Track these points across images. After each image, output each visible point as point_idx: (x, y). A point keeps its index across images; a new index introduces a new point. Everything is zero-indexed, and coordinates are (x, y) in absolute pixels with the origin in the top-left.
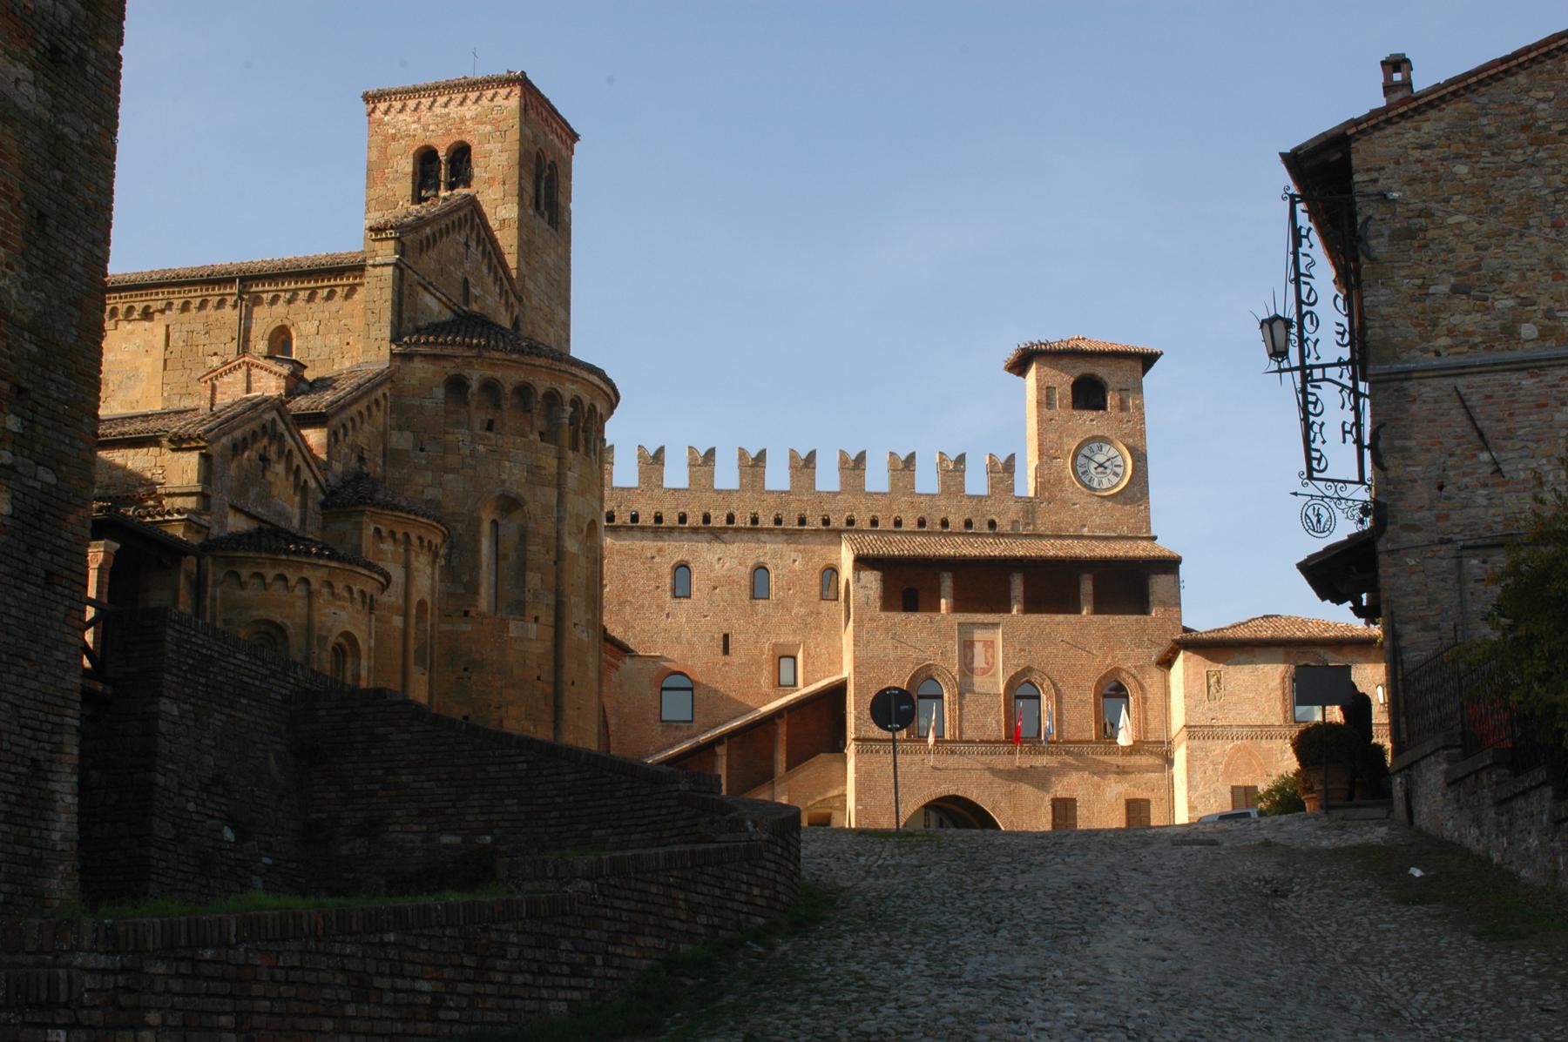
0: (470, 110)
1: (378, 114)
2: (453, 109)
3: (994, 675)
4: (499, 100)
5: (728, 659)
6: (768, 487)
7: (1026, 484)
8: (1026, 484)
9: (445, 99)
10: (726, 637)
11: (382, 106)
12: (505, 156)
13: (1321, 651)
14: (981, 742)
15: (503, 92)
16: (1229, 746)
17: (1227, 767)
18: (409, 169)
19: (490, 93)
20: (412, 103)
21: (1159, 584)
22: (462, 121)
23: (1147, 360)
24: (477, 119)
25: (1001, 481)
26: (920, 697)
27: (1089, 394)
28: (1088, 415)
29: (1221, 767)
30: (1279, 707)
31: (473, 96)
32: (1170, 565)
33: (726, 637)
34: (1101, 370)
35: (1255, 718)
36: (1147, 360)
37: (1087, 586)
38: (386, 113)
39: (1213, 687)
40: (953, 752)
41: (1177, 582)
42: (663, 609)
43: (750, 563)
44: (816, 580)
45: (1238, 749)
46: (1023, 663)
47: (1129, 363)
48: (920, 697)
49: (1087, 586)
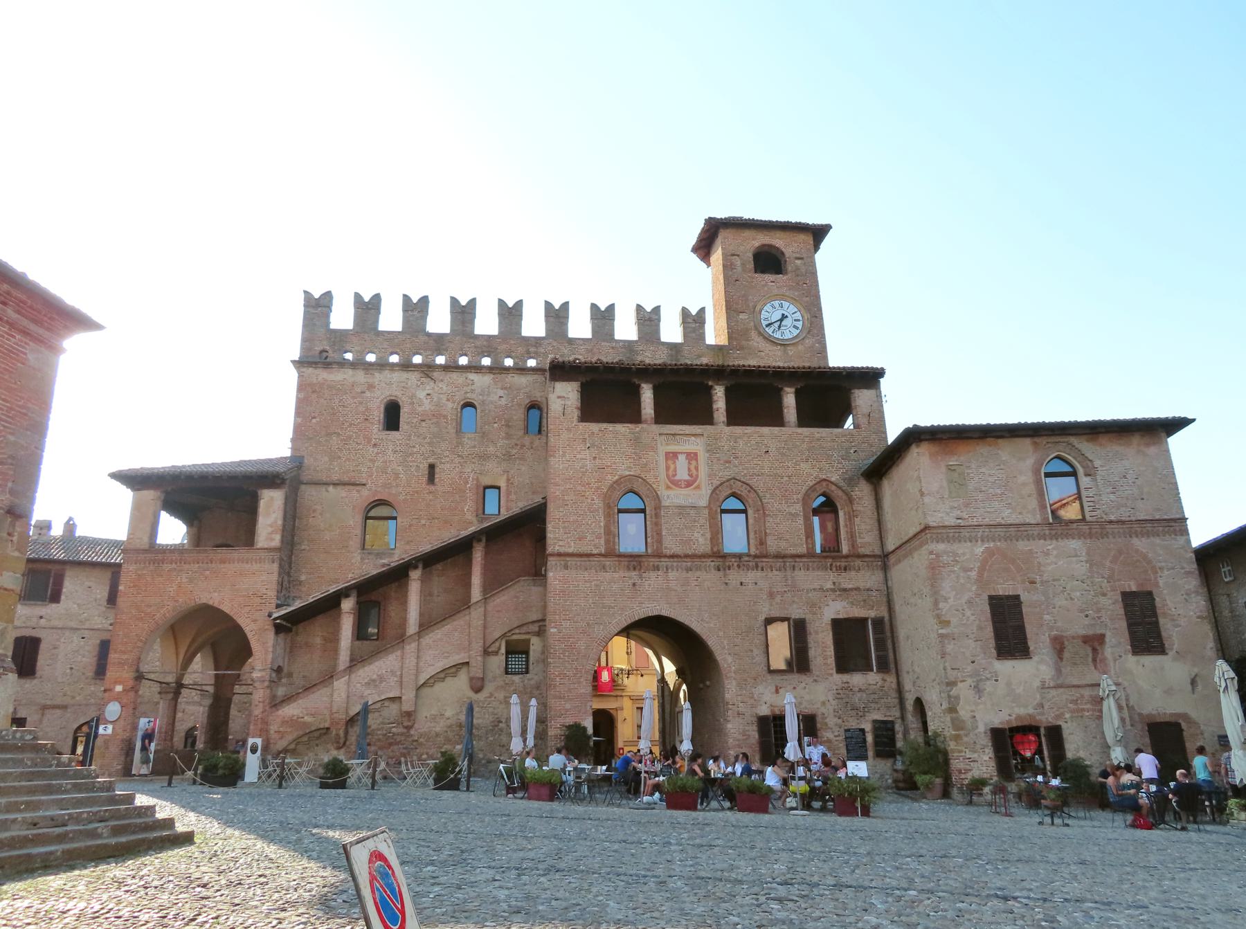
3: (698, 487)
5: (432, 488)
6: (477, 332)
7: (714, 334)
8: (714, 334)
10: (432, 467)
13: (1074, 440)
14: (687, 556)
16: (980, 549)
17: (980, 574)
21: (861, 397)
23: (818, 233)
25: (694, 330)
26: (620, 511)
27: (769, 261)
28: (769, 277)
29: (973, 574)
32: (871, 378)
33: (432, 467)
34: (778, 241)
35: (1009, 516)
36: (818, 233)
37: (789, 400)
39: (957, 483)
40: (657, 568)
41: (879, 396)
42: (369, 441)
43: (460, 398)
44: (519, 415)
45: (990, 553)
46: (727, 474)
47: (802, 237)
48: (620, 511)
49: (789, 400)
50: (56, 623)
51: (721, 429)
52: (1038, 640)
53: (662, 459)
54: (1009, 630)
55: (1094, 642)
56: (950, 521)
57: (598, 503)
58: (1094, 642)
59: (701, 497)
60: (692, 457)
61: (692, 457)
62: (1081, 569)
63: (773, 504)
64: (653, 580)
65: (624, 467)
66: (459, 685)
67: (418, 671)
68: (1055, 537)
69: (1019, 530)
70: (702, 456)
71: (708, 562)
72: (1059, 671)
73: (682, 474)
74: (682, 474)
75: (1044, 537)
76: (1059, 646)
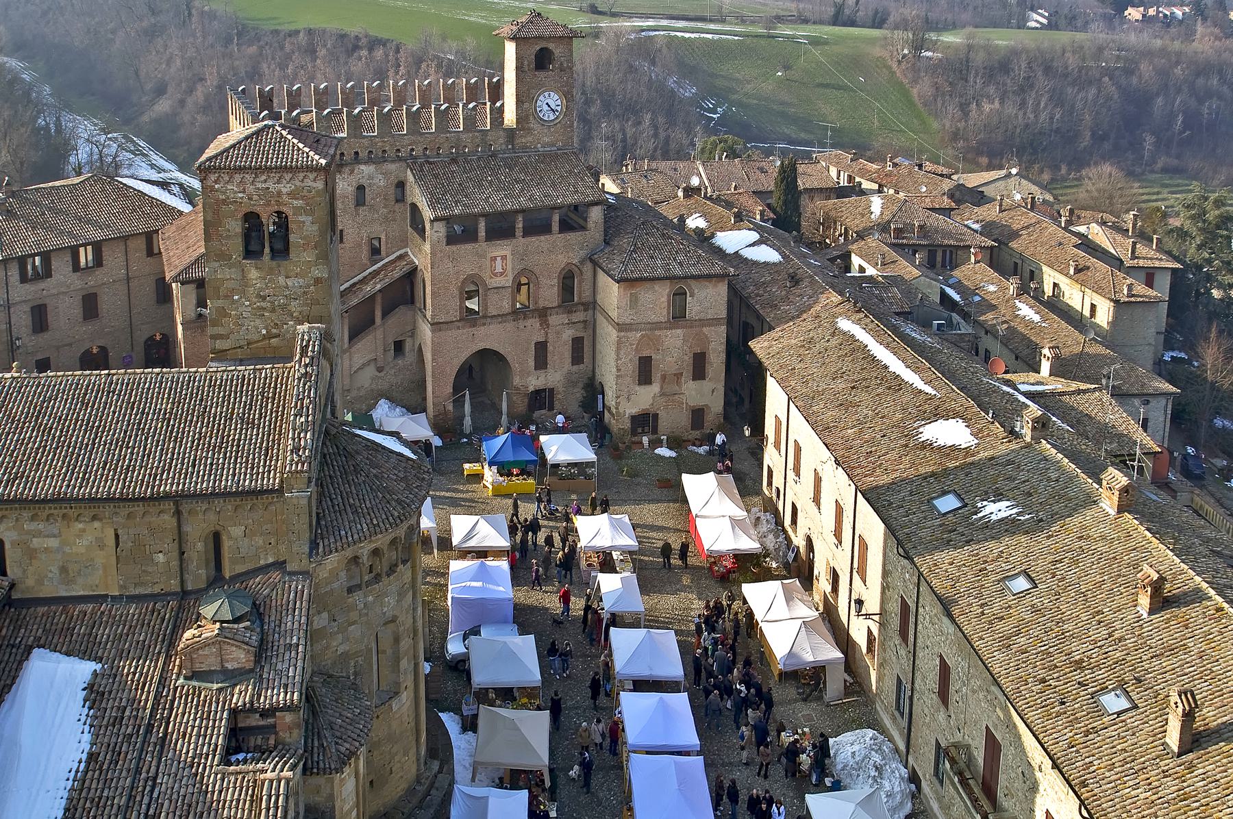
0: (285, 188)
1: (209, 183)
2: (270, 184)
4: (308, 183)
9: (264, 177)
11: (213, 177)
12: (315, 227)
15: (312, 176)
18: (239, 230)
19: (301, 175)
20: (238, 178)
22: (279, 193)
24: (292, 195)
30: (665, 312)
31: (288, 176)
35: (653, 318)
38: (216, 182)
46: (522, 267)
50: (55, 291)
51: (520, 241)
52: (656, 376)
53: (488, 263)
54: (645, 371)
55: (678, 376)
56: (628, 321)
57: (456, 292)
58: (678, 376)
59: (507, 281)
60: (504, 258)
61: (504, 258)
62: (679, 343)
63: (544, 281)
64: (481, 331)
65: (468, 269)
66: (371, 371)
67: (351, 366)
68: (671, 329)
69: (656, 326)
70: (509, 257)
71: (510, 317)
72: (662, 388)
73: (499, 269)
74: (499, 269)
75: (666, 328)
76: (664, 378)
